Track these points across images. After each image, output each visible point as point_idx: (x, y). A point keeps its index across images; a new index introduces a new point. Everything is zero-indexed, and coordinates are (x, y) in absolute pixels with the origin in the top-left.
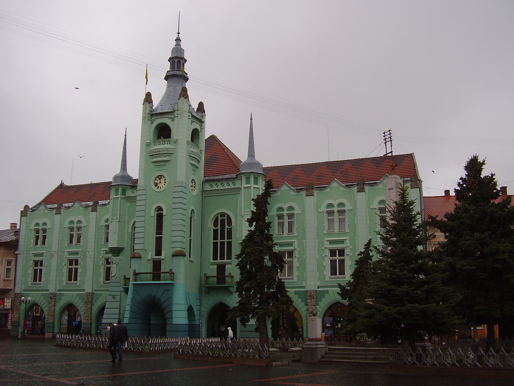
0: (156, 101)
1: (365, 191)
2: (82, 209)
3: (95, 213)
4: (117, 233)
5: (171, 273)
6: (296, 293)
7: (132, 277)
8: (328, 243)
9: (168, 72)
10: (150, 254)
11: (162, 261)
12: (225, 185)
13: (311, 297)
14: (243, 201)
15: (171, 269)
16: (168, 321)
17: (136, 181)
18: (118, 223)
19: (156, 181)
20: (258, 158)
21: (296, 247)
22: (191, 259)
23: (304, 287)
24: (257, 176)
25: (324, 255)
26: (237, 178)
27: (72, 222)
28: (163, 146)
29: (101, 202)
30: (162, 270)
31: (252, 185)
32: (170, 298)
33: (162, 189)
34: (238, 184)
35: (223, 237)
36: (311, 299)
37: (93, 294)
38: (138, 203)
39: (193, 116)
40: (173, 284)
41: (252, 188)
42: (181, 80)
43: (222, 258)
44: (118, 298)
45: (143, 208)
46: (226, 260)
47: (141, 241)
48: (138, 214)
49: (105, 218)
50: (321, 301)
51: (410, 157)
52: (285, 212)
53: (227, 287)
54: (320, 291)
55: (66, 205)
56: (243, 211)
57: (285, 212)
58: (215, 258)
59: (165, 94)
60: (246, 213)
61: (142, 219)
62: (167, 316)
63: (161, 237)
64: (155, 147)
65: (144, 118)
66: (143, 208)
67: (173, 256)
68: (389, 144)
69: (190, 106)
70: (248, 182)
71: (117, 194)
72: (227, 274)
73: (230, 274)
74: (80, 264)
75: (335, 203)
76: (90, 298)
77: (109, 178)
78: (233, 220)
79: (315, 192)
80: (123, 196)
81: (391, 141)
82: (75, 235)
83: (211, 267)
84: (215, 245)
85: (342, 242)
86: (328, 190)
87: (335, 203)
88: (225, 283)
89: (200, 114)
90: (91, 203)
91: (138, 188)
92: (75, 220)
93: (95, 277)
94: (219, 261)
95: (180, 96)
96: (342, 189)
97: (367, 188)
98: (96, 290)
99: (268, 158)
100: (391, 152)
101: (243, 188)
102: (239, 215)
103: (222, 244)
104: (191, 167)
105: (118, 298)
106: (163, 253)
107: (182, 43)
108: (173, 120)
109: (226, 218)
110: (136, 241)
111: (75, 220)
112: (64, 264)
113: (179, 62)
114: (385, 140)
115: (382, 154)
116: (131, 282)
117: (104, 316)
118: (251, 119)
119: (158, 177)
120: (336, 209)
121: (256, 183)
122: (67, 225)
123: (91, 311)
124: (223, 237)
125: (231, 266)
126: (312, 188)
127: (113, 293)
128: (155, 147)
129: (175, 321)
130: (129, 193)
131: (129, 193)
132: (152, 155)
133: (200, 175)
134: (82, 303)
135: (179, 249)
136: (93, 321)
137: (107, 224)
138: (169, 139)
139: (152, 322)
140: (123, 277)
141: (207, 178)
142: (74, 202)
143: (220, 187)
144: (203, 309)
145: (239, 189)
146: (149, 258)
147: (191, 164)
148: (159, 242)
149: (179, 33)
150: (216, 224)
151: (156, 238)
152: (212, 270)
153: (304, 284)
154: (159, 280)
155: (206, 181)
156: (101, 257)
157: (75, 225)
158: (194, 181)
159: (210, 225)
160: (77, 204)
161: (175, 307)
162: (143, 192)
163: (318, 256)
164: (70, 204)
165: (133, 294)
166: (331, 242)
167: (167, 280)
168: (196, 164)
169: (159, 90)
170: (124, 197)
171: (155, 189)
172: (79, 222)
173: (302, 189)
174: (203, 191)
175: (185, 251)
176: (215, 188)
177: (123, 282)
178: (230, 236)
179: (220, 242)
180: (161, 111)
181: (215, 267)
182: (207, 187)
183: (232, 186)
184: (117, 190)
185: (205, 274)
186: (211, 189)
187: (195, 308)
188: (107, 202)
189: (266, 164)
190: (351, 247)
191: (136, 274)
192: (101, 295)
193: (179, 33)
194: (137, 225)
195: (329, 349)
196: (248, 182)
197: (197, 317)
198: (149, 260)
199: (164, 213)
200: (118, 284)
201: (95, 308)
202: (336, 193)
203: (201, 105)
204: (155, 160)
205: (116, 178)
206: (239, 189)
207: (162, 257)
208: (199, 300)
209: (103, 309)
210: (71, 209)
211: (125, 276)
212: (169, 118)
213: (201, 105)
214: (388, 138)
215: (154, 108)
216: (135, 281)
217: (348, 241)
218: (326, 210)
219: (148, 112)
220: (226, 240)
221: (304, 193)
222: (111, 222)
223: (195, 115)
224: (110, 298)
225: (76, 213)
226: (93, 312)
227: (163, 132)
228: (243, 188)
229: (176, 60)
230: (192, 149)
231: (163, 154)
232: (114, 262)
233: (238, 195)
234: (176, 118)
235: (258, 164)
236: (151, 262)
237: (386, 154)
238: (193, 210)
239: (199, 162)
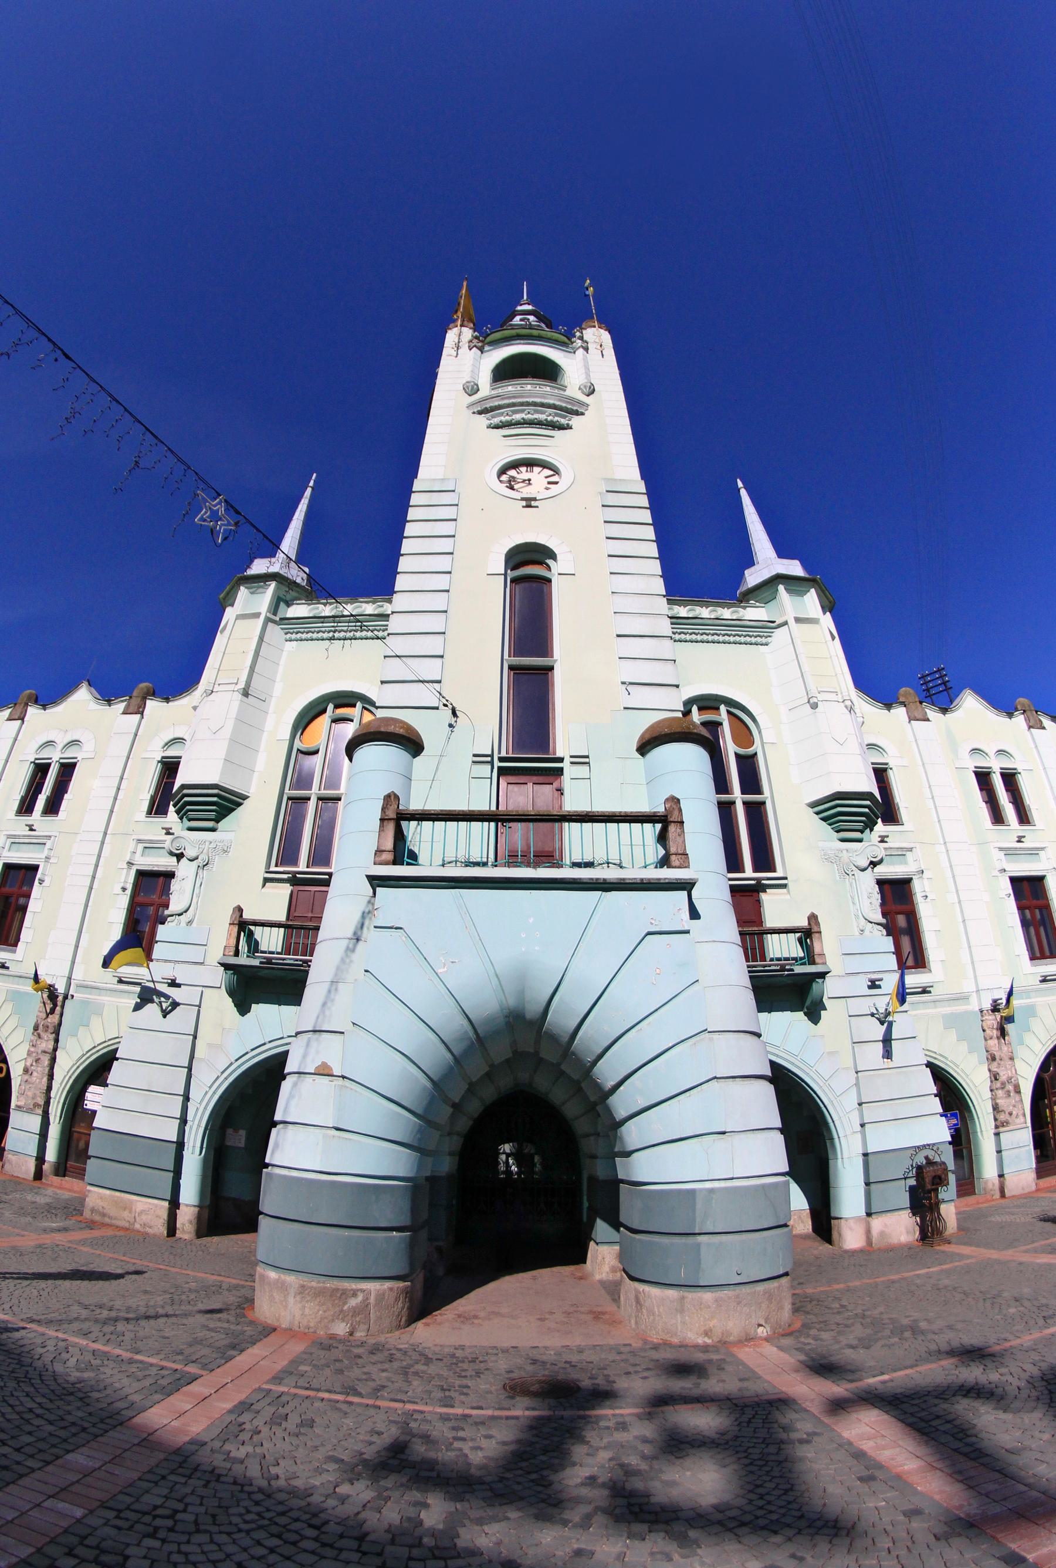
4: (227, 732)
27: (49, 743)
67: (645, 747)
73: (813, 918)
140: (226, 916)
157: (55, 756)
201: (69, 1063)
211: (240, 910)
231: (543, 405)
232: (190, 852)
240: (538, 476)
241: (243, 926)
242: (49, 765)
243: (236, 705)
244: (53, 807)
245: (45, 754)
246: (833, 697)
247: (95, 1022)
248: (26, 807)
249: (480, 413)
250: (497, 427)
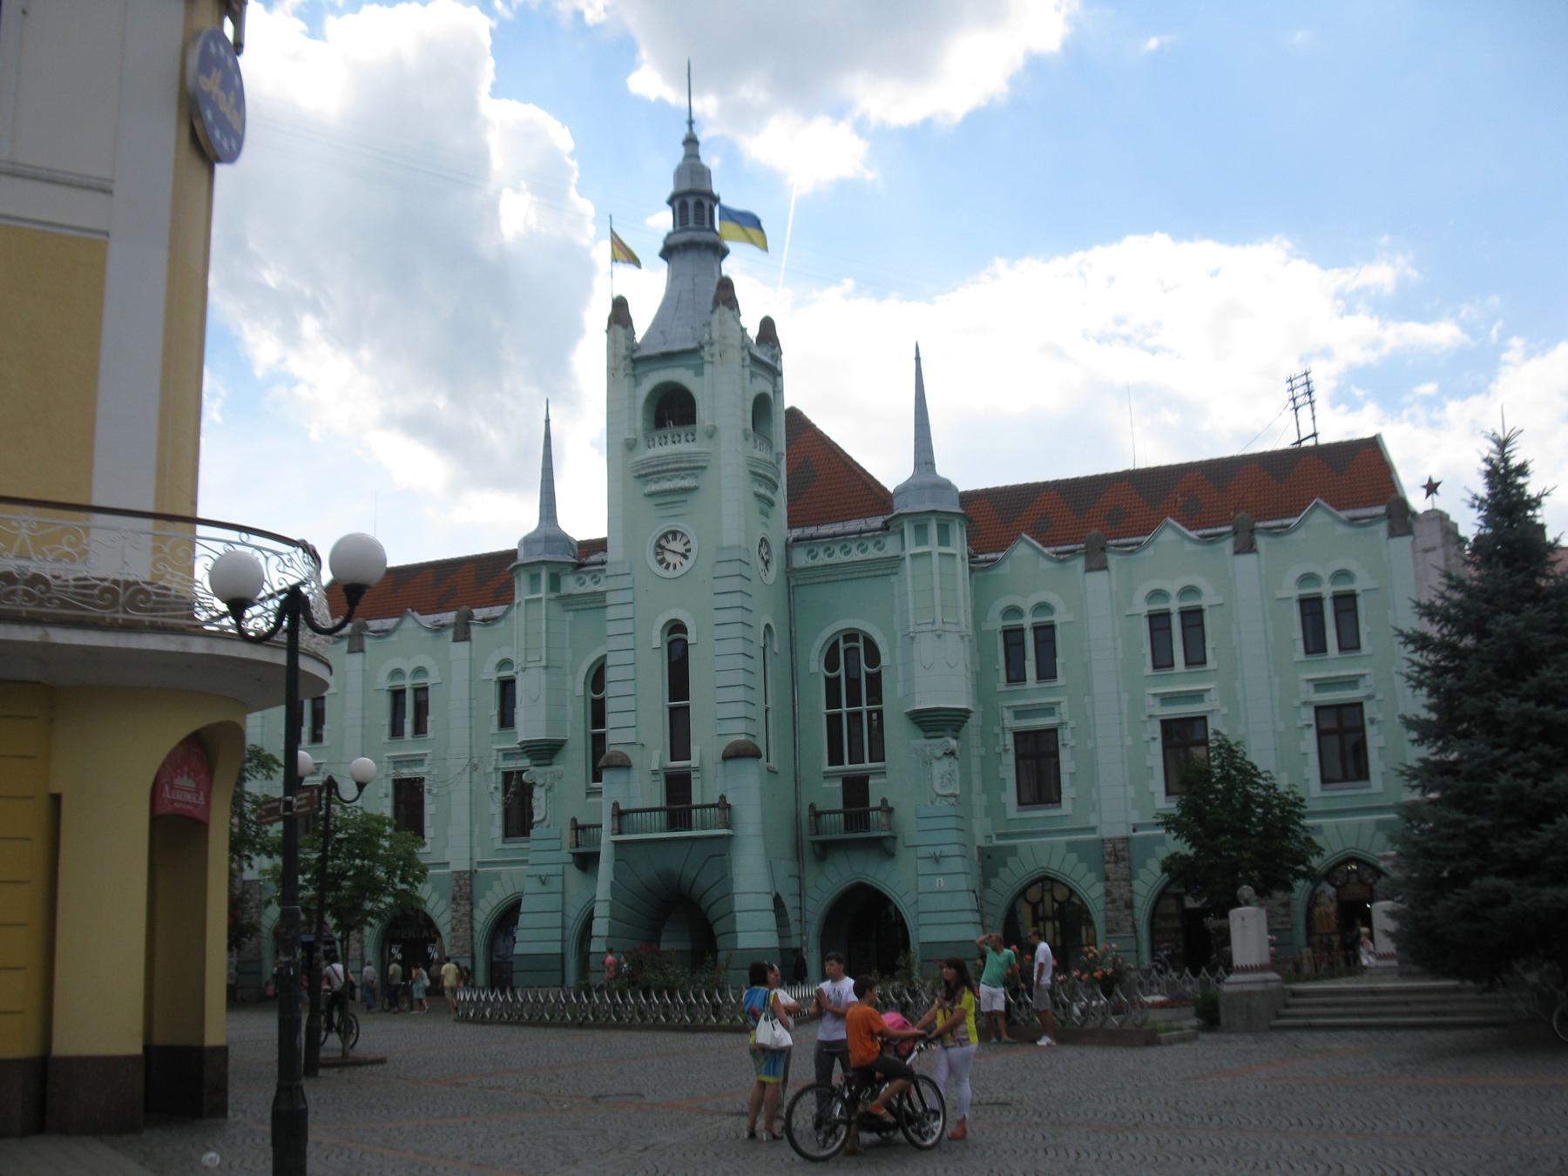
0: (642, 321)
1: (1255, 551)
2: (424, 634)
3: (466, 644)
5: (723, 805)
6: (1071, 846)
7: (607, 822)
8: (1157, 700)
9: (669, 235)
10: (656, 754)
11: (693, 775)
12: (854, 548)
13: (1117, 858)
14: (910, 597)
15: (723, 797)
16: (721, 942)
17: (599, 546)
18: (543, 671)
20: (944, 469)
21: (1066, 717)
22: (771, 764)
23: (1093, 830)
24: (944, 521)
25: (1147, 737)
26: (886, 527)
27: (397, 673)
28: (670, 447)
29: (479, 613)
30: (696, 800)
31: (933, 546)
32: (726, 878)
33: (680, 571)
34: (891, 547)
35: (854, 700)
36: (1116, 863)
37: (472, 873)
38: (611, 613)
39: (755, 360)
40: (729, 837)
41: (935, 557)
42: (710, 256)
43: (856, 758)
44: (556, 883)
45: (627, 627)
46: (868, 765)
47: (630, 719)
48: (613, 644)
49: (497, 657)
50: (1144, 866)
51: (1372, 447)
52: (1027, 622)
53: (879, 840)
54: (1141, 838)
55: (375, 624)
56: (912, 619)
57: (1027, 622)
58: (835, 758)
59: (667, 299)
60: (923, 628)
61: (628, 657)
62: (718, 928)
63: (687, 707)
64: (651, 453)
65: (612, 371)
66: (627, 627)
67: (728, 757)
68: (1305, 412)
69: (743, 330)
70: (921, 537)
71: (534, 587)
72: (874, 802)
73: (884, 801)
74: (429, 791)
75: (1173, 587)
76: (465, 888)
77: (510, 544)
79: (1113, 560)
80: (553, 595)
81: (1312, 402)
82: (409, 708)
83: (826, 785)
84: (833, 722)
85: (1197, 696)
86: (1150, 552)
87: (1173, 587)
88: (866, 826)
89: (765, 348)
90: (449, 617)
91: (609, 569)
92: (408, 668)
93: (477, 828)
94: (847, 766)
95: (716, 303)
96: (1189, 547)
97: (1261, 542)
98: (481, 864)
99: (970, 468)
100: (1315, 435)
101: (908, 559)
103: (855, 717)
104: (755, 505)
105: (556, 883)
106: (695, 750)
107: (702, 151)
108: (699, 371)
109: (861, 645)
110: (611, 720)
111: (408, 668)
112: (382, 792)
113: (699, 205)
114: (1294, 400)
115: (1284, 442)
116: (607, 838)
117: (520, 934)
118: (918, 359)
119: (665, 536)
120: (1174, 606)
121: (944, 539)
122: (384, 683)
123: (471, 923)
124: (854, 700)
125: (883, 781)
126: (1103, 549)
127: (543, 870)
128: (651, 453)
129: (745, 941)
130: (570, 585)
131: (570, 585)
132: (646, 475)
133: (778, 527)
134: (443, 904)
135: (743, 738)
136: (480, 951)
137: (506, 673)
138: (689, 428)
139: (664, 946)
141: (796, 532)
142: (399, 613)
143: (839, 557)
144: (810, 904)
145: (895, 562)
146: (655, 767)
147: (757, 495)
148: (679, 723)
149: (691, 122)
150: (831, 661)
151: (672, 710)
152: (830, 795)
153: (1093, 821)
154: (690, 828)
155: (797, 540)
156: (490, 769)
157: (408, 683)
158: (767, 544)
159: (815, 663)
160: (408, 623)
161: (740, 903)
162: (625, 582)
163: (1129, 741)
164: (389, 623)
165: (617, 872)
166: (1167, 699)
167: (715, 827)
168: (769, 494)
169: (648, 288)
170: (558, 598)
171: (660, 570)
172: (420, 671)
173: (1072, 552)
174: (790, 571)
175: (760, 743)
176: (823, 559)
177: (568, 836)
178: (875, 693)
179: (849, 714)
180: (664, 349)
181: (838, 784)
182: (801, 559)
183: (873, 553)
184: (535, 578)
185: (812, 806)
186: (811, 563)
187: (789, 903)
188: (497, 611)
189: (965, 484)
190: (1224, 711)
191: (619, 814)
192: (497, 876)
193: (691, 122)
194: (610, 674)
195: (1295, 994)
196: (921, 537)
197: (794, 928)
198: (655, 773)
199: (691, 639)
200: (556, 844)
202: (1172, 562)
203: (767, 326)
204: (654, 487)
205: (527, 542)
206: (895, 562)
207: (694, 762)
208: (795, 882)
209: (508, 916)
210: (394, 638)
211: (574, 820)
212: (688, 367)
213: (767, 326)
214: (1302, 392)
215: (638, 338)
216: (620, 833)
217: (1213, 695)
218: (1143, 608)
219: (623, 351)
220: (865, 707)
221: (1079, 563)
222: (524, 670)
223: (758, 353)
224: (532, 885)
225: (409, 646)
226: (478, 927)
227: (672, 409)
228: (908, 559)
229: (691, 201)
230: (758, 454)
231: (677, 470)
232: (540, 781)
233: (893, 579)
234: (707, 369)
235: (947, 486)
236: (662, 777)
237: (1299, 442)
238: (768, 627)
239: (776, 487)
240: (677, 546)
241: (577, 828)
242: (403, 691)
243: (543, 677)
244: (420, 728)
245: (398, 683)
246: (929, 627)
247: (497, 886)
248: (396, 731)
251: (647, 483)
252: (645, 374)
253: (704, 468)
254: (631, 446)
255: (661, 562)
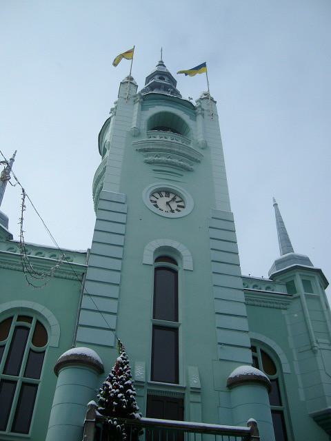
11: (189, 398)
19: (155, 199)
63: (176, 330)
78: (283, 358)
102: (294, 352)
118: (276, 205)
151: (155, 327)
212: (186, 113)
231: (179, 154)
233: (284, 312)
234: (200, 117)
249: (140, 150)
250: (149, 163)
251: (147, 156)
252: (153, 106)
253: (199, 162)
254: (136, 133)
255: (156, 206)
